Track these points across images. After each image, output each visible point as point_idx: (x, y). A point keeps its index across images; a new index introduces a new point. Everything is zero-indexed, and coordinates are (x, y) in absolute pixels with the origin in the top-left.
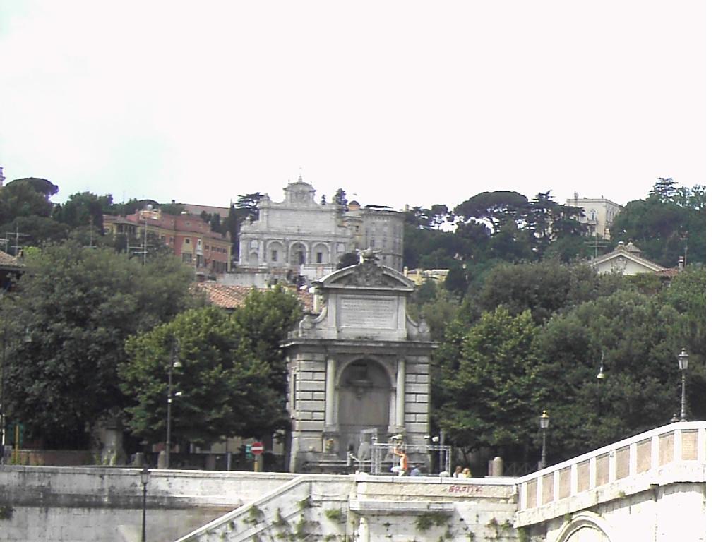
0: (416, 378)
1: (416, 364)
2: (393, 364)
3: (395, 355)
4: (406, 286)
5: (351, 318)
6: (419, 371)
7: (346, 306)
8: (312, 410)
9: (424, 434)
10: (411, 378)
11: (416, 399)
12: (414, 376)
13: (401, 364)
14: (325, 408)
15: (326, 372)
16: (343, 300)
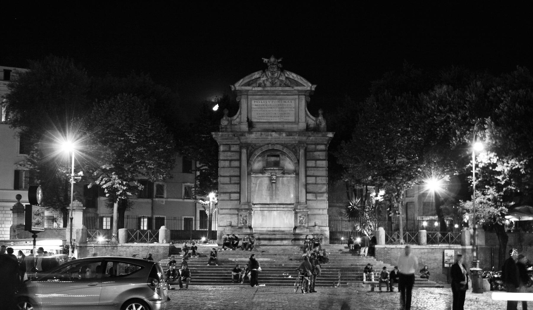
0: (316, 164)
1: (315, 151)
5: (260, 115)
6: (318, 157)
7: (256, 105)
8: (230, 191)
9: (323, 209)
10: (311, 164)
12: (314, 162)
14: (240, 189)
15: (240, 160)
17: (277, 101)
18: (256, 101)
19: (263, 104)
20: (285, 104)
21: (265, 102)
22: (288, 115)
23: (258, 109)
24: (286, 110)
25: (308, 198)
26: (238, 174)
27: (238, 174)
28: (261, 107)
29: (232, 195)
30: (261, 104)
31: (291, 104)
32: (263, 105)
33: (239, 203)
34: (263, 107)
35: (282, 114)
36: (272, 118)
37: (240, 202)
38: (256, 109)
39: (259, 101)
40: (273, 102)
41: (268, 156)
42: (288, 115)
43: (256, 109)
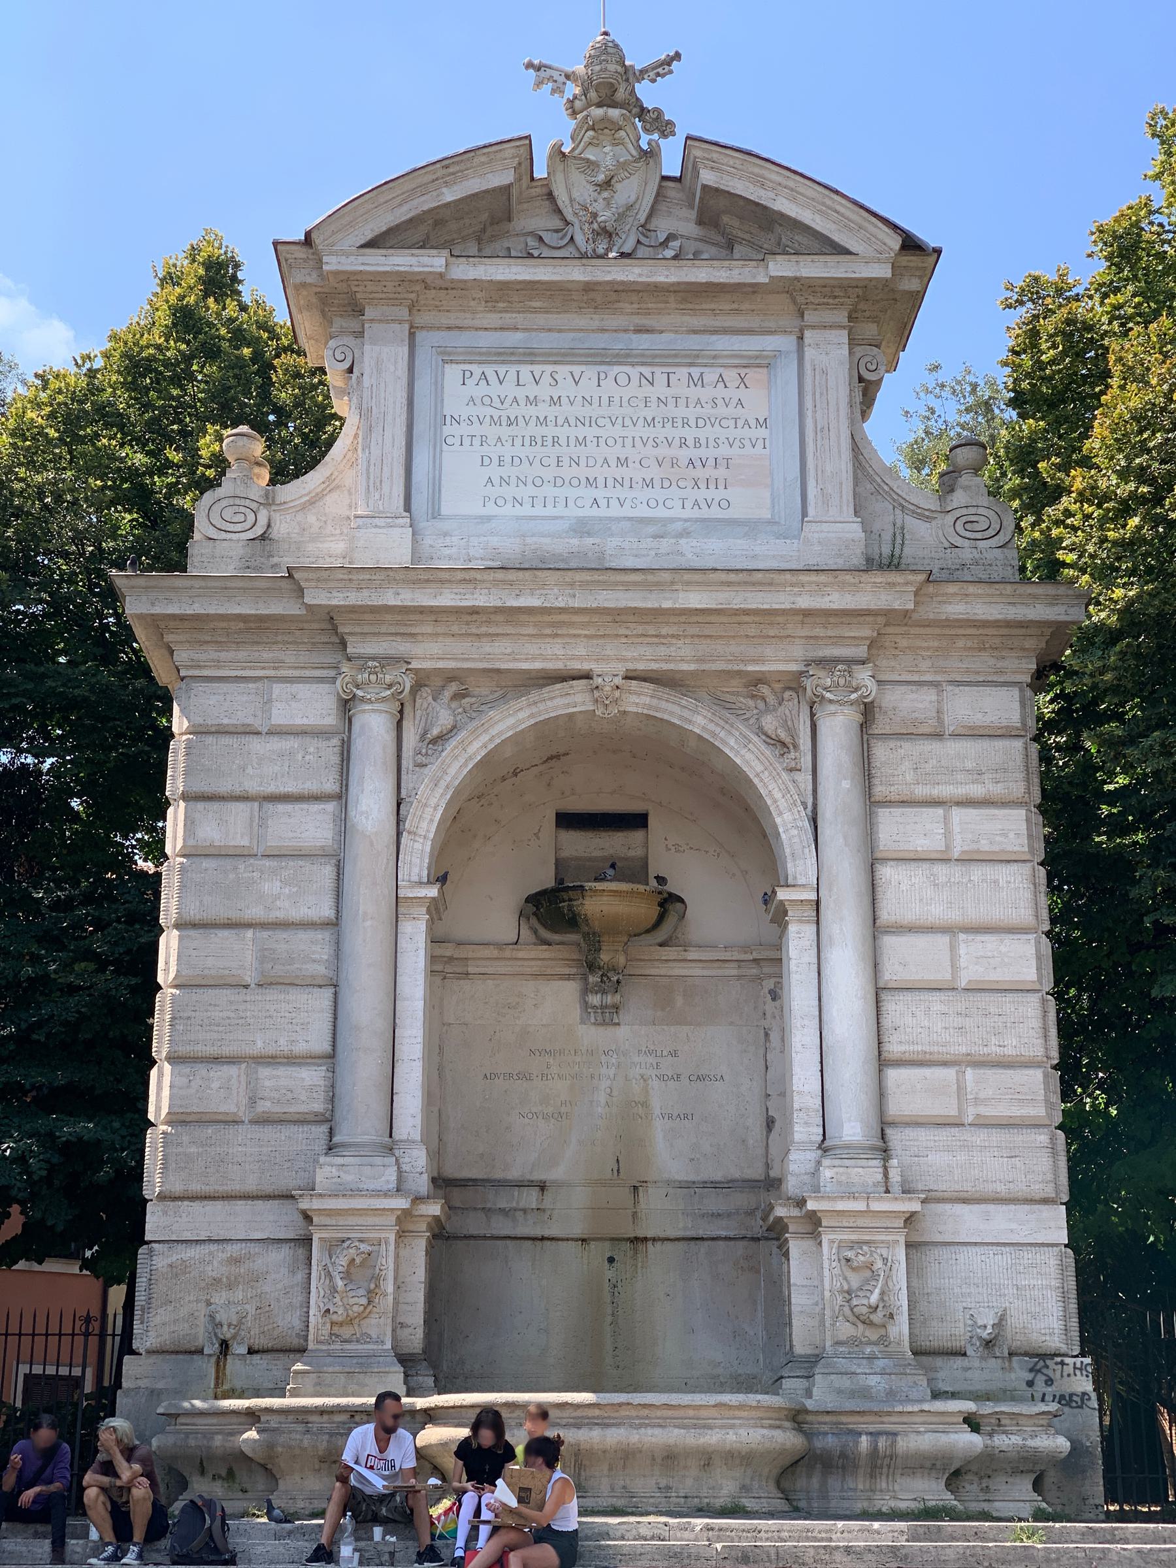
2: (782, 746)
4: (848, 252)
16: (453, 373)
17: (634, 372)
18: (477, 369)
19: (531, 390)
20: (694, 392)
21: (546, 379)
22: (721, 472)
23: (492, 432)
24: (702, 434)
25: (892, 972)
26: (327, 912)
27: (327, 912)
29: (271, 1079)
31: (742, 393)
32: (533, 401)
33: (321, 1145)
34: (532, 411)
36: (600, 494)
38: (476, 429)
39: (502, 370)
40: (608, 383)
42: (721, 472)
43: (476, 429)
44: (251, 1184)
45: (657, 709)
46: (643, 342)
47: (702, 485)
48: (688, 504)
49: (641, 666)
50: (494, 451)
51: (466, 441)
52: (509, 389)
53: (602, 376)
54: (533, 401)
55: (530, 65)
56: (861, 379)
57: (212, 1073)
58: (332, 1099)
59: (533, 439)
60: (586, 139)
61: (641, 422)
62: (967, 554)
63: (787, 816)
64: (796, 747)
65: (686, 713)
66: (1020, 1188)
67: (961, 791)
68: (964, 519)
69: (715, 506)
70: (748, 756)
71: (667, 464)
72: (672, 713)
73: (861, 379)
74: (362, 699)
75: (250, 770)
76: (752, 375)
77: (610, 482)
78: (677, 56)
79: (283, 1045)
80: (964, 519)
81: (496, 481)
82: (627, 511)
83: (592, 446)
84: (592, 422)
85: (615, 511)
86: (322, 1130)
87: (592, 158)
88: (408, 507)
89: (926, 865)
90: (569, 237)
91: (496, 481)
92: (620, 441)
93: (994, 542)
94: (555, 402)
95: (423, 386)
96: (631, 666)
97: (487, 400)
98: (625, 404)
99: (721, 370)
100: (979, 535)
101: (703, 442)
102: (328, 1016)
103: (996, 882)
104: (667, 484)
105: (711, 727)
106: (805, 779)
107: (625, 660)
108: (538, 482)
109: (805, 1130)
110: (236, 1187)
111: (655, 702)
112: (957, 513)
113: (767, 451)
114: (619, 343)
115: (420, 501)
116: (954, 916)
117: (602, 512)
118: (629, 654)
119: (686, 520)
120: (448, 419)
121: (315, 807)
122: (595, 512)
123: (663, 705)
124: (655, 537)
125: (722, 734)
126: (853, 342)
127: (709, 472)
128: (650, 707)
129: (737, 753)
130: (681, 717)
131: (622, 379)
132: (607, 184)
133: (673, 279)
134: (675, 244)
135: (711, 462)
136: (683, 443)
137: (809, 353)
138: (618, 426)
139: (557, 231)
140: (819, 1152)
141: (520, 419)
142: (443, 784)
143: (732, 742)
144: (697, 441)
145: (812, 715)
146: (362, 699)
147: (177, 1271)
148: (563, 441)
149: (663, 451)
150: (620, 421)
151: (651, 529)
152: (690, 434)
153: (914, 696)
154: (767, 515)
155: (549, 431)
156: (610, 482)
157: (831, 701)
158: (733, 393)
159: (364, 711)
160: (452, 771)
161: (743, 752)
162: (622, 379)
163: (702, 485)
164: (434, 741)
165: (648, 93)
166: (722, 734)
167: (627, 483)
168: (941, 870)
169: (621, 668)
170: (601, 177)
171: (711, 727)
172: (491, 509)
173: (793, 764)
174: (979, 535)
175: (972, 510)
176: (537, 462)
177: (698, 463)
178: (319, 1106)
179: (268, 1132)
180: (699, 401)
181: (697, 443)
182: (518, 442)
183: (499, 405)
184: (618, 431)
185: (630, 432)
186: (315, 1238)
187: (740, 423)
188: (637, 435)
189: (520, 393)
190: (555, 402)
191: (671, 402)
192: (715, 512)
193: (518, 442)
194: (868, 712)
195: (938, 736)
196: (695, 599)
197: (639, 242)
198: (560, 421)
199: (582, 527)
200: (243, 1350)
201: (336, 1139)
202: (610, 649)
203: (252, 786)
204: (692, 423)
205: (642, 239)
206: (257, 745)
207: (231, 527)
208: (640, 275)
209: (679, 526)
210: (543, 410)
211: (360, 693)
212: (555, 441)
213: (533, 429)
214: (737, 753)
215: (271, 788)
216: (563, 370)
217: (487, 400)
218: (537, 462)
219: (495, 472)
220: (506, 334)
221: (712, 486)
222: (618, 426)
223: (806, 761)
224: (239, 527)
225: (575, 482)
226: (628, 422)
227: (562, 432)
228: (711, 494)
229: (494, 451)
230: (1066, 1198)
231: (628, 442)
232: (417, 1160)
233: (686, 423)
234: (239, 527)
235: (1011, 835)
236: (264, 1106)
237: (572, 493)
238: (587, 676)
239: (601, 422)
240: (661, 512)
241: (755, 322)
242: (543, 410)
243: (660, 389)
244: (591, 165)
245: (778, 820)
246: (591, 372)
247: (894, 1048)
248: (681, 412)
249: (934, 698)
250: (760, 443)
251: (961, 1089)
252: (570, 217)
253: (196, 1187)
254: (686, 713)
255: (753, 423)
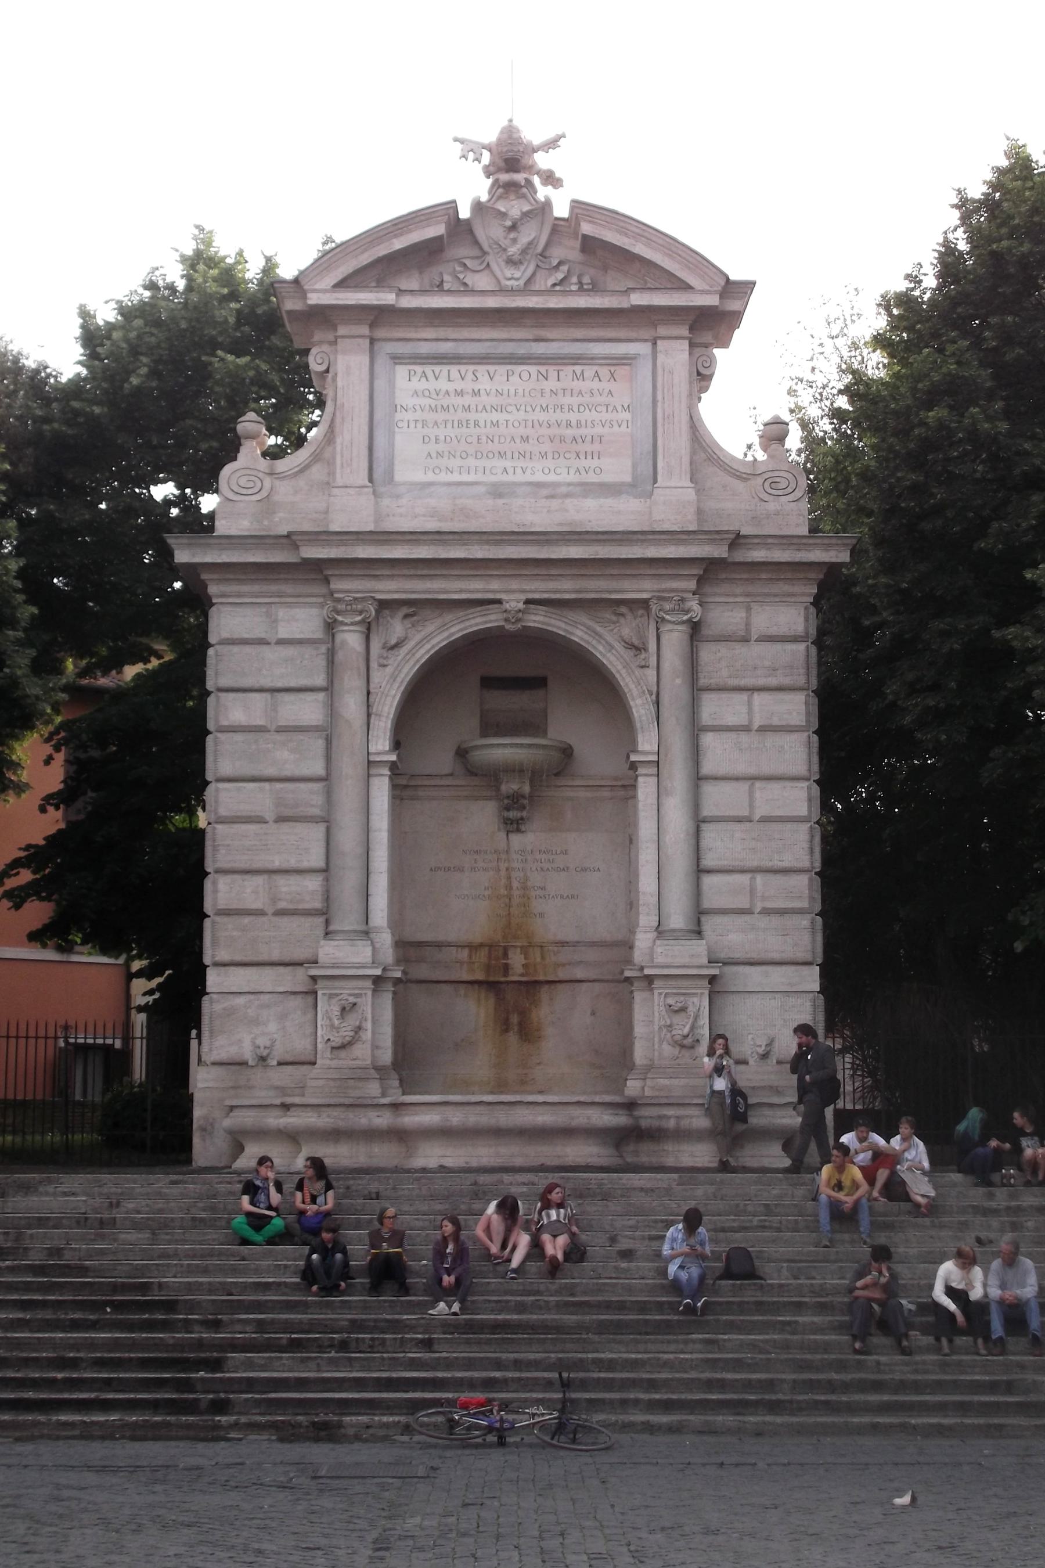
2: (638, 649)
3: (645, 604)
11: (751, 806)
13: (674, 639)
16: (401, 371)
17: (533, 369)
18: (419, 369)
19: (459, 385)
20: (577, 385)
21: (470, 376)
22: (597, 447)
23: (431, 417)
28: (445, 402)
29: (287, 886)
30: (443, 385)
32: (460, 393)
33: (320, 932)
34: (459, 401)
35: (562, 440)
36: (508, 464)
37: (327, 922)
38: (418, 415)
40: (515, 379)
41: (488, 683)
42: (597, 447)
44: (276, 956)
45: (549, 625)
46: (540, 348)
47: (582, 457)
48: (572, 472)
49: (537, 596)
50: (432, 432)
51: (412, 425)
52: (443, 385)
53: (510, 373)
54: (460, 393)
55: (456, 140)
56: (699, 374)
57: (246, 883)
58: (327, 898)
59: (460, 422)
60: (498, 194)
61: (538, 409)
62: (772, 506)
63: (639, 701)
64: (646, 650)
65: (569, 628)
66: (789, 954)
67: (761, 682)
68: (770, 480)
69: (591, 472)
70: (612, 658)
71: (557, 440)
72: (559, 628)
73: (699, 374)
74: (342, 623)
75: (264, 672)
76: (621, 371)
77: (516, 455)
78: (563, 136)
79: (293, 863)
80: (770, 480)
81: (434, 455)
82: (529, 477)
83: (503, 427)
84: (502, 409)
85: (519, 477)
86: (320, 920)
87: (503, 210)
88: (371, 480)
89: (733, 735)
90: (485, 264)
91: (434, 455)
92: (523, 423)
93: (791, 497)
94: (476, 393)
95: (380, 384)
96: (530, 596)
97: (427, 393)
98: (527, 394)
99: (596, 368)
100: (780, 493)
101: (583, 423)
102: (322, 844)
103: (782, 747)
104: (556, 456)
105: (586, 637)
106: (651, 673)
107: (523, 591)
108: (464, 455)
109: (647, 919)
110: (264, 957)
111: (547, 620)
112: (766, 476)
113: (629, 430)
114: (522, 349)
115: (378, 474)
116: (752, 771)
117: (510, 478)
118: (527, 588)
119: (569, 484)
120: (399, 407)
121: (309, 697)
122: (505, 478)
123: (553, 621)
124: (547, 497)
125: (594, 642)
126: (692, 345)
127: (588, 447)
128: (543, 623)
129: (604, 656)
130: (565, 630)
131: (525, 376)
132: (513, 228)
133: (561, 306)
134: (565, 268)
135: (589, 438)
136: (569, 425)
137: (661, 358)
138: (522, 412)
139: (477, 258)
140: (655, 934)
141: (451, 408)
142: (399, 679)
143: (601, 648)
144: (579, 423)
145: (658, 629)
146: (342, 623)
147: (230, 1013)
148: (482, 424)
149: (555, 431)
150: (523, 408)
151: (545, 492)
152: (573, 417)
153: (730, 614)
154: (628, 478)
155: (472, 416)
156: (516, 455)
157: (670, 622)
158: (605, 386)
159: (343, 631)
160: (405, 670)
161: (609, 655)
162: (525, 376)
163: (582, 457)
164: (392, 648)
165: (542, 160)
166: (594, 642)
167: (528, 455)
168: (744, 737)
169: (523, 597)
170: (509, 223)
171: (586, 637)
172: (430, 477)
173: (643, 663)
174: (780, 493)
175: (776, 474)
176: (463, 441)
177: (579, 440)
178: (318, 905)
179: (284, 921)
180: (580, 392)
181: (579, 424)
182: (449, 425)
183: (435, 396)
184: (521, 415)
185: (531, 416)
186: (320, 993)
187: (610, 409)
188: (535, 418)
189: (451, 387)
190: (476, 393)
191: (561, 392)
192: (592, 478)
193: (449, 425)
194: (695, 628)
195: (745, 640)
196: (575, 552)
197: (538, 266)
198: (480, 408)
199: (497, 491)
200: (275, 1063)
201: (331, 928)
202: (514, 585)
203: (267, 683)
204: (576, 409)
205: (540, 264)
206: (270, 653)
207: (245, 492)
208: (537, 303)
209: (564, 490)
210: (467, 400)
211: (340, 618)
212: (476, 424)
213: (461, 415)
214: (604, 656)
215: (280, 684)
216: (481, 369)
217: (427, 393)
218: (463, 441)
219: (433, 448)
220: (439, 343)
221: (589, 457)
222: (522, 412)
223: (653, 660)
224: (250, 492)
225: (490, 455)
226: (529, 409)
227: (482, 417)
228: (588, 463)
229: (432, 432)
230: (820, 961)
231: (530, 424)
232: (385, 940)
233: (570, 409)
234: (250, 492)
235: (795, 714)
236: (282, 905)
237: (488, 464)
238: (499, 602)
239: (509, 409)
240: (552, 478)
241: (622, 333)
242: (467, 400)
243: (552, 384)
244: (504, 215)
245: (632, 703)
246: (502, 369)
247: (708, 862)
248: (567, 400)
249: (744, 615)
250: (624, 425)
251: (752, 891)
252: (486, 247)
253: (238, 958)
254: (569, 628)
255: (619, 408)
